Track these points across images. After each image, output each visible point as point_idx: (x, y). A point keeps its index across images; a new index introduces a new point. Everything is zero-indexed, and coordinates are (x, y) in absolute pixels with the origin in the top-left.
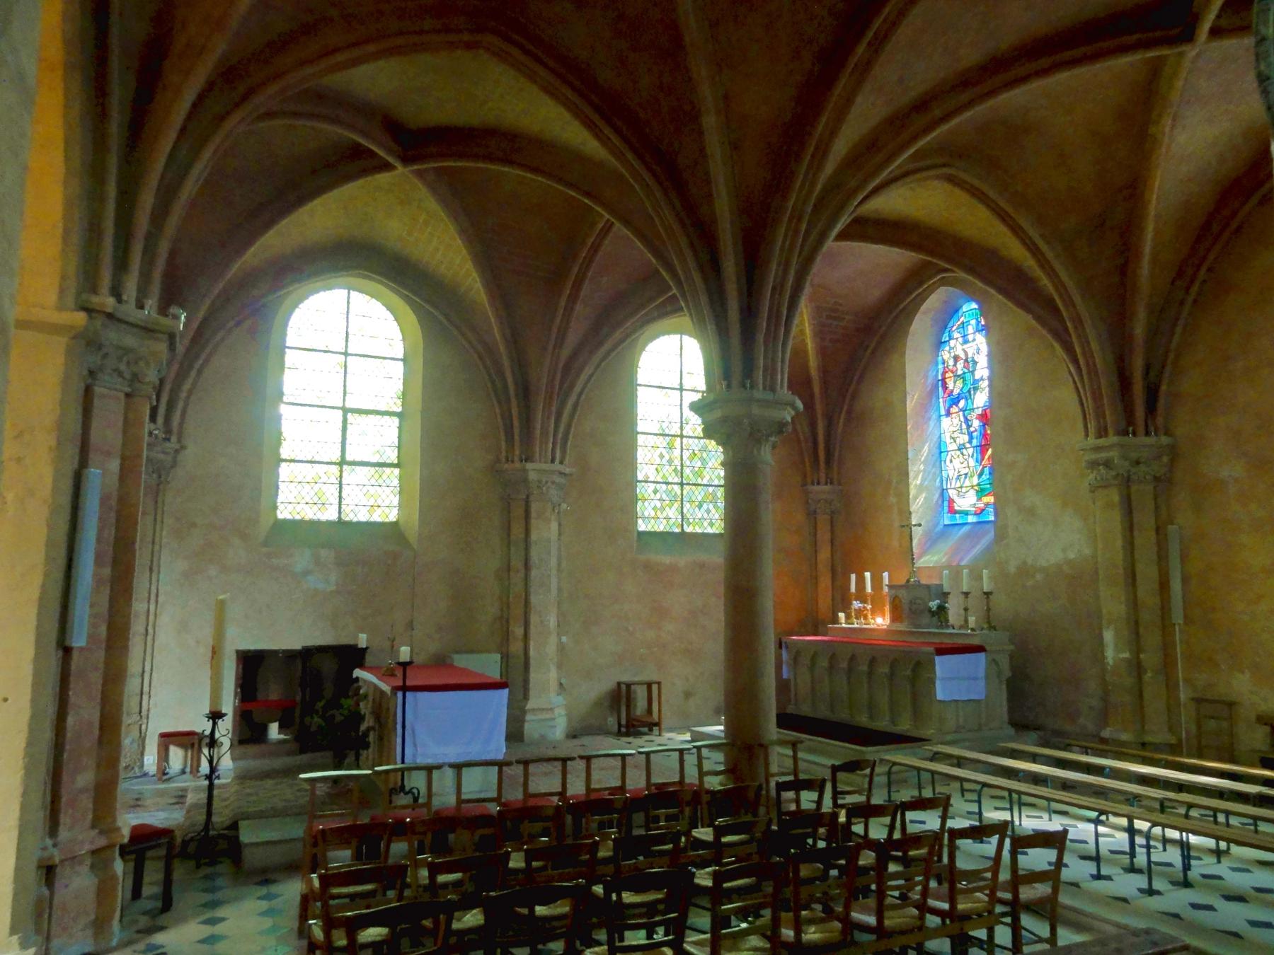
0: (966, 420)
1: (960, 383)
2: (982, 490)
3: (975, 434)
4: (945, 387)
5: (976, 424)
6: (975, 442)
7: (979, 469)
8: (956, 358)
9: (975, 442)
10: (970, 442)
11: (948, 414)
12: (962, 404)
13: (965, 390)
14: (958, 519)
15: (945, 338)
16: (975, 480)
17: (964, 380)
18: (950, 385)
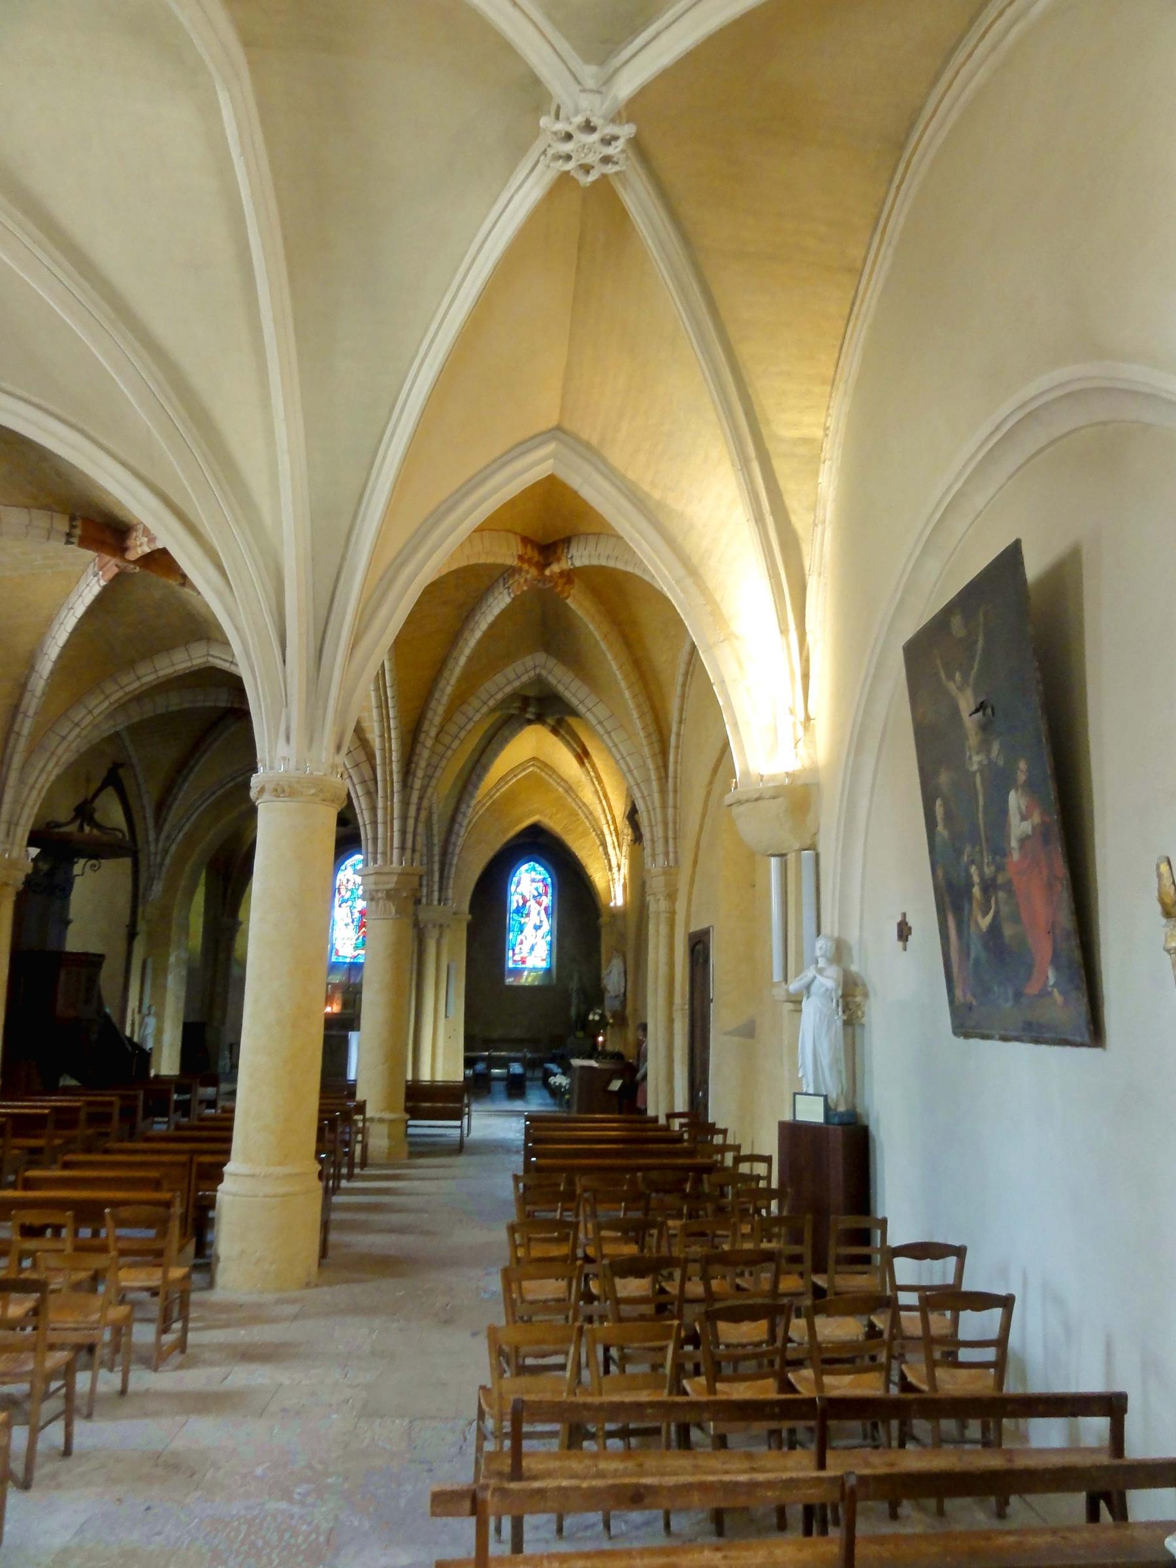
0: (351, 912)
1: (349, 893)
2: (357, 947)
3: (355, 920)
4: (340, 893)
5: (357, 915)
6: (355, 923)
7: (357, 936)
8: (348, 880)
9: (355, 923)
10: (353, 922)
11: (340, 906)
12: (350, 903)
13: (352, 897)
14: (341, 960)
15: (343, 867)
16: (354, 941)
17: (352, 892)
18: (343, 891)
